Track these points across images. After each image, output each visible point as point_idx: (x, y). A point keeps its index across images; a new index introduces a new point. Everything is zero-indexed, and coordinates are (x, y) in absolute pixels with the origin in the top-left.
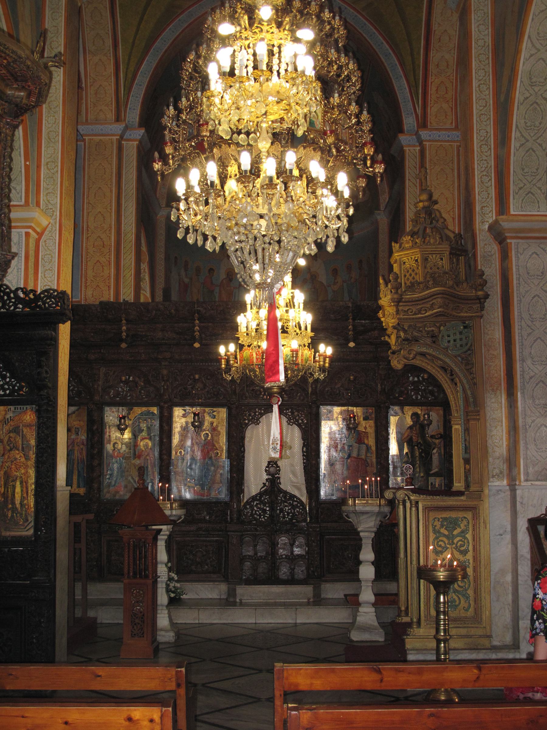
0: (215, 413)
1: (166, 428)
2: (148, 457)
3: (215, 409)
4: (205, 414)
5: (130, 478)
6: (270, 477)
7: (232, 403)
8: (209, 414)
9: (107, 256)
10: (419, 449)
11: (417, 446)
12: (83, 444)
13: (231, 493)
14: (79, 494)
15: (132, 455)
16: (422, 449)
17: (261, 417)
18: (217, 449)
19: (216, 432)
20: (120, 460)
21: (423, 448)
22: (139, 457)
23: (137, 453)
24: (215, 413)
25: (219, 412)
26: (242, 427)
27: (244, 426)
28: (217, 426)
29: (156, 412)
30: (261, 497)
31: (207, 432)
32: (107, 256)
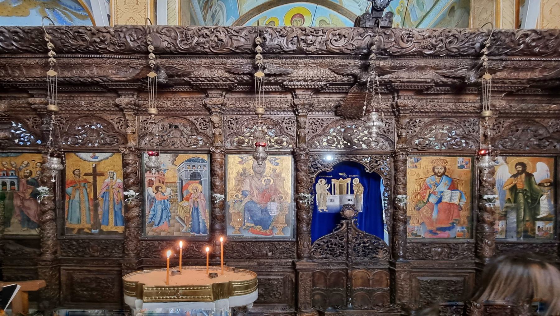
1: (219, 171)
2: (198, 200)
7: (302, 149)
10: (524, 195)
11: (522, 193)
12: (119, 187)
14: (117, 232)
16: (527, 196)
18: (280, 193)
20: (164, 202)
21: (529, 194)
22: (188, 199)
23: (184, 196)
28: (281, 172)
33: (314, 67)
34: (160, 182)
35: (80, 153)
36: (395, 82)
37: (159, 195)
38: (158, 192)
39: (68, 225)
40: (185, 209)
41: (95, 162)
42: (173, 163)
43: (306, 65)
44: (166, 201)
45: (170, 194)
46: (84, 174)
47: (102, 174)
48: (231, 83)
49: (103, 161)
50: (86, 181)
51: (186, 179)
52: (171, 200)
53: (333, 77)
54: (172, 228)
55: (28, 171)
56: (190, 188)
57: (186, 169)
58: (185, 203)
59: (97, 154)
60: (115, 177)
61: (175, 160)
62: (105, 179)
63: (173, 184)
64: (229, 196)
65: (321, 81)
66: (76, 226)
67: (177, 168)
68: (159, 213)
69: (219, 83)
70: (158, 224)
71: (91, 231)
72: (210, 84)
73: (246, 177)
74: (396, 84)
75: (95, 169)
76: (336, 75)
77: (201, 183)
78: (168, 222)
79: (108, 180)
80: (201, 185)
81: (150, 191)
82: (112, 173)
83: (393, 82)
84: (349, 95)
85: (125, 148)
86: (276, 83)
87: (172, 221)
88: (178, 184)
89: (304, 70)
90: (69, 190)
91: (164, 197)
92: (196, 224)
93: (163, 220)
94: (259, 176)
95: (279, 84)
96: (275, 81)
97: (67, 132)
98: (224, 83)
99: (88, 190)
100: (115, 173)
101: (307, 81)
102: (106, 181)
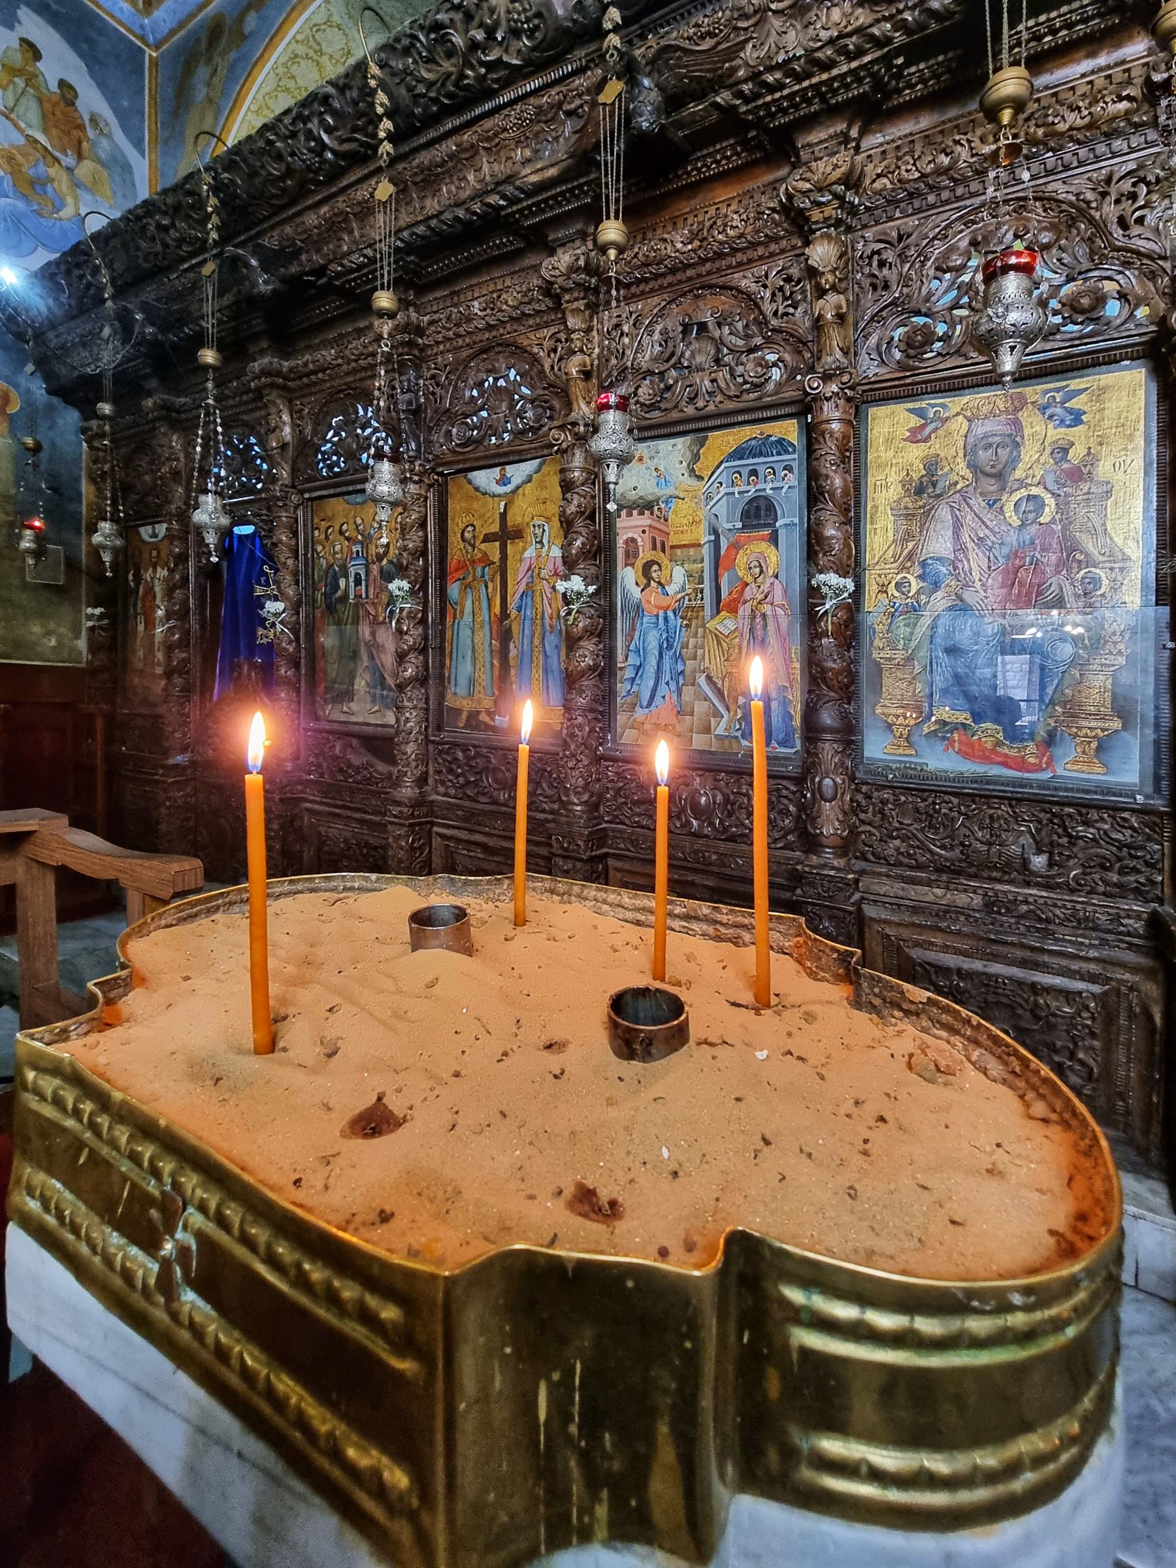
0: (1073, 404)
3: (1075, 384)
4: (1023, 416)
8: (1043, 409)
22: (733, 610)
23: (724, 594)
24: (1074, 403)
25: (1103, 390)
28: (1091, 458)
31: (1035, 491)
34: (654, 548)
35: (475, 473)
37: (653, 597)
38: (648, 585)
39: (450, 701)
40: (724, 645)
45: (683, 589)
46: (481, 537)
47: (518, 534)
50: (486, 561)
52: (689, 613)
56: (741, 560)
59: (510, 470)
60: (545, 541)
62: (524, 549)
63: (692, 551)
64: (871, 587)
66: (465, 703)
67: (702, 487)
70: (649, 705)
71: (493, 720)
73: (938, 496)
75: (503, 516)
77: (774, 539)
78: (675, 696)
79: (530, 553)
80: (777, 546)
81: (628, 578)
88: (706, 552)
91: (665, 601)
94: (991, 486)
97: (449, 410)
102: (527, 554)
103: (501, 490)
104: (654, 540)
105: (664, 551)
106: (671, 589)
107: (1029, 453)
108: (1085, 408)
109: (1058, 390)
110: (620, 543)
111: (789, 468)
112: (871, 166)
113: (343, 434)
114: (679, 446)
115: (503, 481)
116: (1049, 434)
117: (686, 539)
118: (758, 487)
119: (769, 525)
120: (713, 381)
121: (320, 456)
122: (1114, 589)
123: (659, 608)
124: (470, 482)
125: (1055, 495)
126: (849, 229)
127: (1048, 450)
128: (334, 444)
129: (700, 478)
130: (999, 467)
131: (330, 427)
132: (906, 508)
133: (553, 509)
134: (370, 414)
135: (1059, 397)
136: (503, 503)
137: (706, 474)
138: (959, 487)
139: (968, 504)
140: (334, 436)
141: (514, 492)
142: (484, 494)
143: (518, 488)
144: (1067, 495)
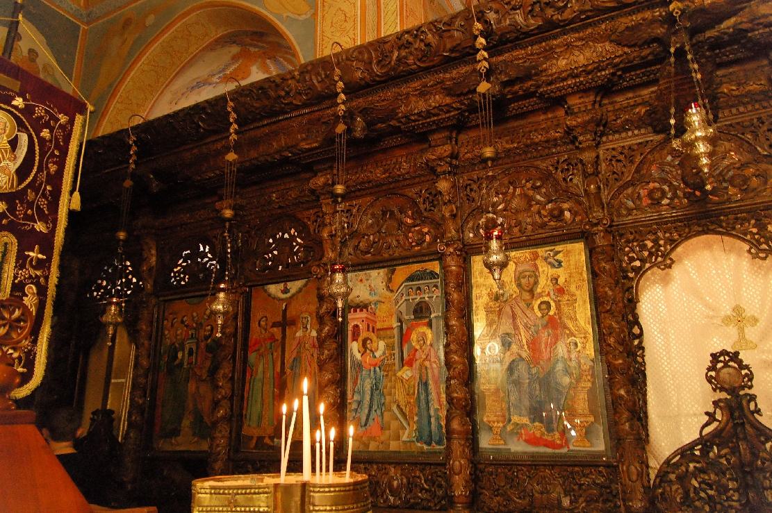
0: (559, 257)
2: (427, 363)
3: (558, 248)
4: (538, 262)
5: (394, 408)
6: (724, 395)
7: (595, 221)
8: (546, 259)
9: (351, 32)
12: (314, 346)
13: (616, 438)
15: (397, 361)
17: (673, 250)
19: (566, 297)
20: (375, 371)
22: (410, 363)
24: (559, 257)
26: (626, 277)
27: (631, 275)
29: (437, 270)
30: (705, 452)
31: (546, 299)
32: (351, 32)
33: (584, 45)
34: (368, 330)
36: (753, 30)
38: (365, 351)
40: (406, 386)
41: (287, 298)
42: (389, 287)
43: (569, 47)
44: (377, 369)
45: (384, 353)
46: (271, 324)
47: (293, 323)
48: (457, 112)
49: (295, 297)
50: (272, 338)
51: (407, 317)
53: (621, 56)
54: (387, 432)
55: (209, 327)
56: (414, 336)
57: (407, 298)
58: (406, 373)
60: (309, 327)
61: (390, 280)
62: (296, 332)
63: (388, 332)
65: (604, 70)
68: (368, 397)
69: (440, 117)
72: (428, 123)
74: (757, 32)
76: (626, 49)
77: (430, 325)
81: (354, 347)
82: (305, 318)
83: (746, 31)
84: (661, 83)
85: (319, 266)
86: (528, 95)
87: (387, 414)
88: (396, 332)
89: (567, 57)
90: (252, 357)
92: (425, 421)
93: (373, 415)
95: (533, 94)
96: (524, 91)
98: (447, 115)
99: (275, 354)
100: (309, 319)
101: (577, 76)
102: (298, 334)
103: (284, 296)
104: (368, 326)
105: (373, 332)
106: (378, 354)
107: (543, 281)
108: (562, 260)
109: (551, 251)
110: (350, 328)
111: (436, 286)
112: (462, 149)
113: (189, 262)
114: (381, 274)
115: (285, 291)
116: (550, 271)
117: (386, 325)
118: (422, 296)
119: (426, 317)
120: (397, 241)
121: (172, 275)
122: (584, 348)
123: (370, 365)
124: (266, 291)
125: (555, 301)
126: (455, 174)
127: (550, 279)
128: (183, 267)
129: (392, 291)
130: (531, 287)
131: (182, 257)
132: (491, 307)
133: (313, 308)
134: (207, 250)
135: (552, 254)
136: (284, 304)
137: (395, 288)
138: (514, 296)
139: (519, 306)
140: (183, 262)
141: (291, 297)
142: (274, 298)
143: (293, 295)
144: (559, 301)
